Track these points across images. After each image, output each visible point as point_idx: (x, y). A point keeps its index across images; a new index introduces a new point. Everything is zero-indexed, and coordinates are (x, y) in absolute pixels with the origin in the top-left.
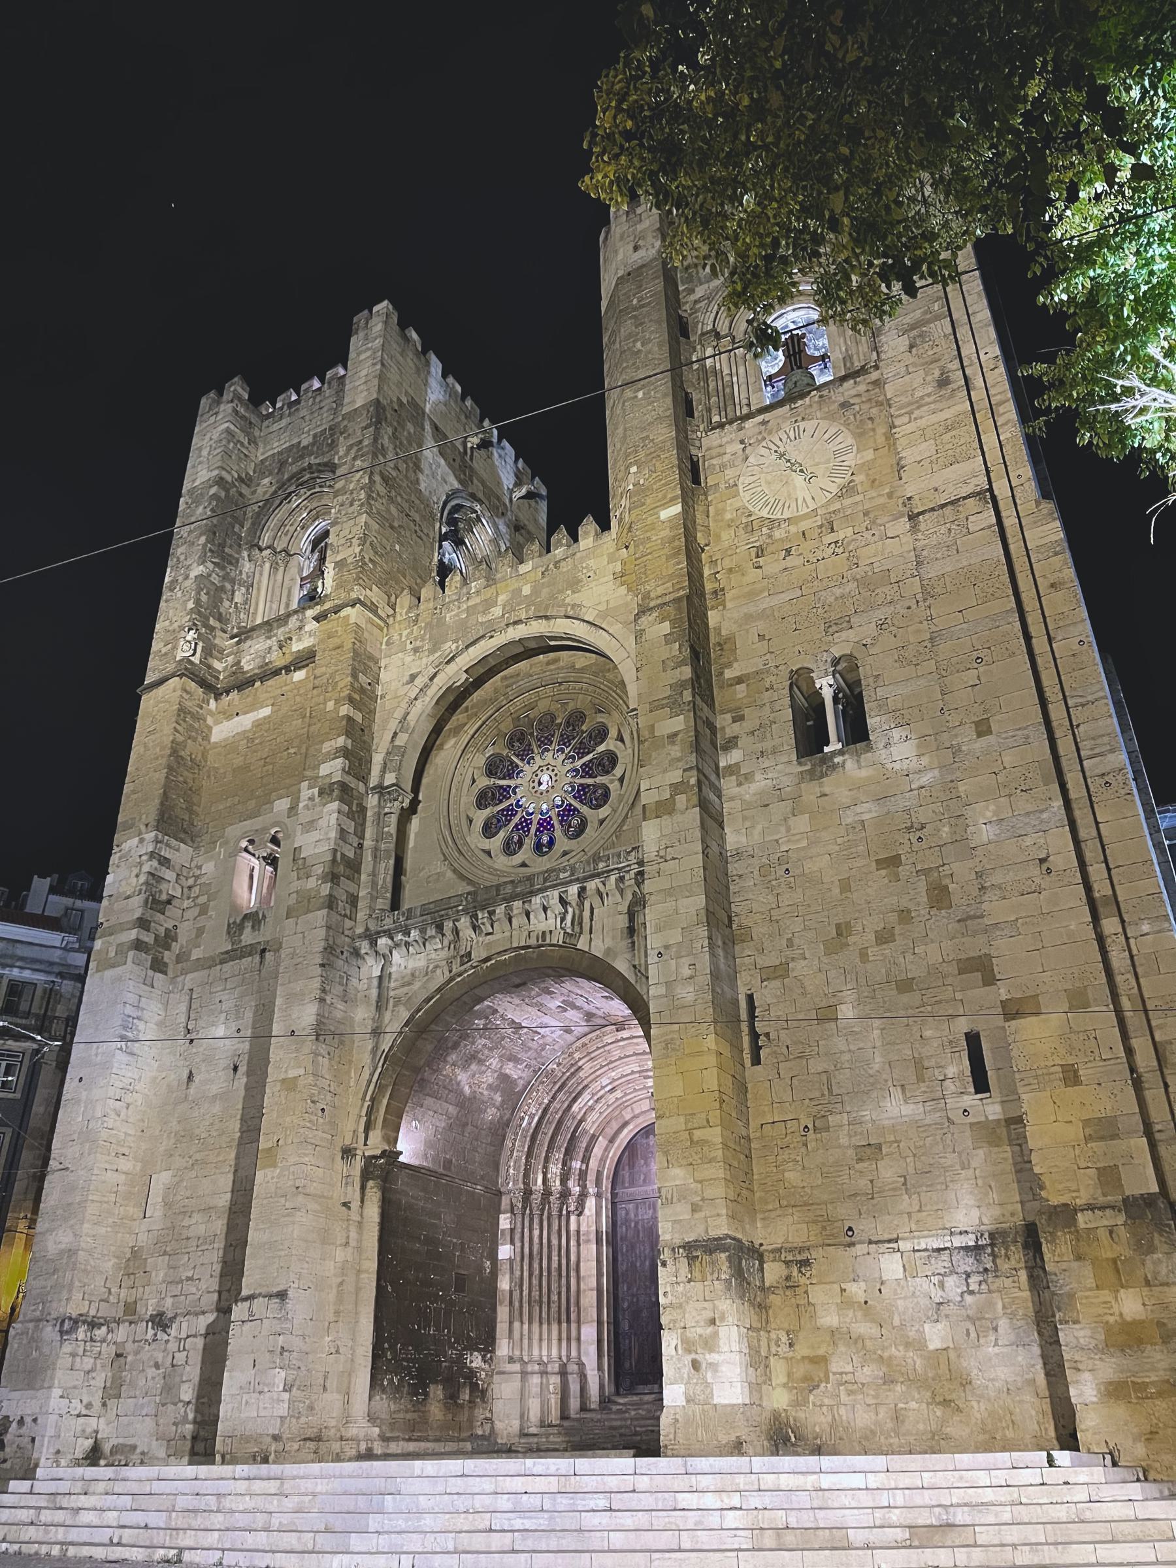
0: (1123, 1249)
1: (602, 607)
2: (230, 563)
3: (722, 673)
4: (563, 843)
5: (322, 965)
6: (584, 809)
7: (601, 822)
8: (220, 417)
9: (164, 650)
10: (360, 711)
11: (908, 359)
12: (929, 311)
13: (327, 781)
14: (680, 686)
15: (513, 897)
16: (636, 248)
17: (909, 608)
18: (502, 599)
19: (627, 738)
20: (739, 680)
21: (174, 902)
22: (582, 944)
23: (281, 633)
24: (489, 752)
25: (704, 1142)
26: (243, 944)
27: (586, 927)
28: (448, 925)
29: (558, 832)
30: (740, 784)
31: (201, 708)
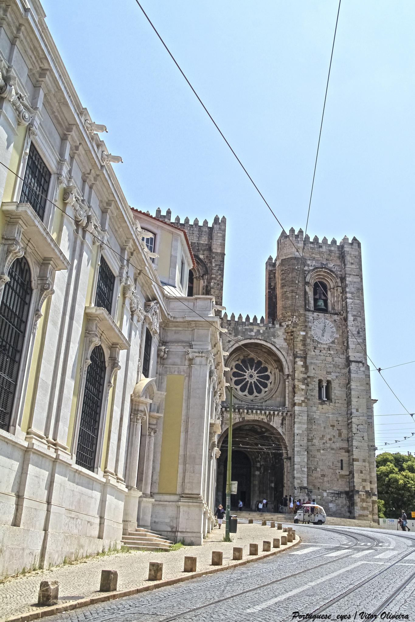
0: (364, 497)
1: (281, 346)
4: (255, 394)
6: (262, 387)
7: (266, 392)
11: (353, 323)
12: (358, 314)
15: (258, 409)
18: (255, 330)
19: (273, 372)
20: (308, 377)
22: (271, 424)
24: (237, 362)
25: (303, 471)
27: (272, 420)
28: (241, 410)
29: (255, 391)
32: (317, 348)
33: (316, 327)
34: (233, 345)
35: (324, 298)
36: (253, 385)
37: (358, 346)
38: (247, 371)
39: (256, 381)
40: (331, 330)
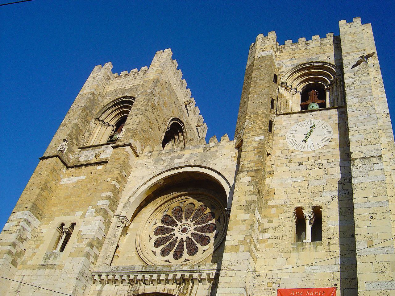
2: (87, 122)
3: (267, 203)
4: (186, 255)
5: (78, 279)
6: (198, 245)
7: (204, 251)
8: (100, 73)
9: (54, 146)
10: (120, 184)
11: (357, 105)
13: (99, 208)
14: (251, 202)
16: (263, 50)
17: (345, 194)
20: (273, 207)
21: (27, 240)
23: (98, 150)
24: (165, 213)
26: (49, 263)
28: (132, 277)
29: (185, 252)
30: (266, 247)
31: (60, 170)
32: (292, 162)
33: (294, 132)
34: (147, 181)
35: (321, 101)
36: (185, 243)
37: (369, 134)
38: (178, 223)
39: (190, 236)
40: (324, 130)
